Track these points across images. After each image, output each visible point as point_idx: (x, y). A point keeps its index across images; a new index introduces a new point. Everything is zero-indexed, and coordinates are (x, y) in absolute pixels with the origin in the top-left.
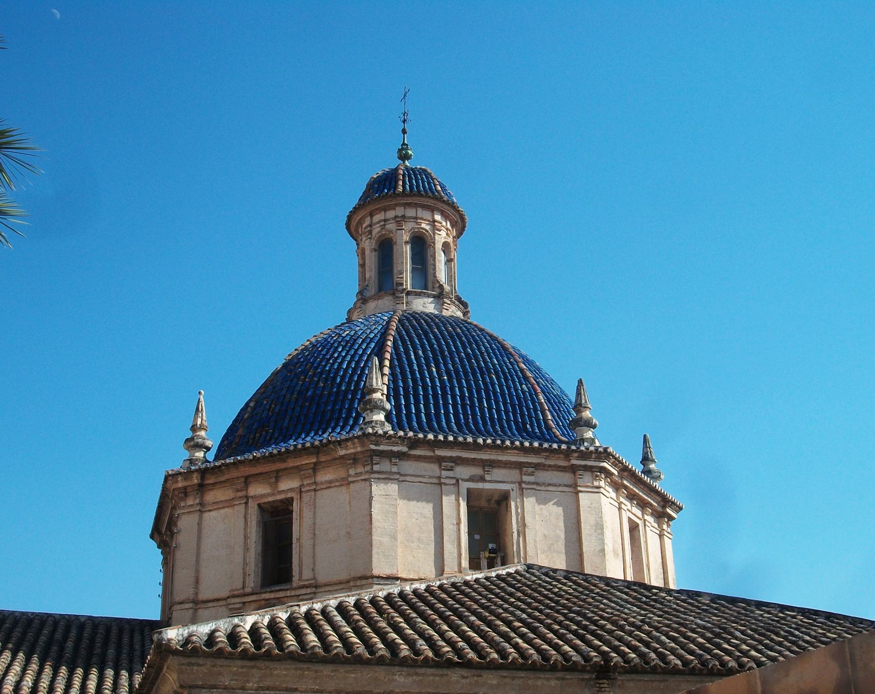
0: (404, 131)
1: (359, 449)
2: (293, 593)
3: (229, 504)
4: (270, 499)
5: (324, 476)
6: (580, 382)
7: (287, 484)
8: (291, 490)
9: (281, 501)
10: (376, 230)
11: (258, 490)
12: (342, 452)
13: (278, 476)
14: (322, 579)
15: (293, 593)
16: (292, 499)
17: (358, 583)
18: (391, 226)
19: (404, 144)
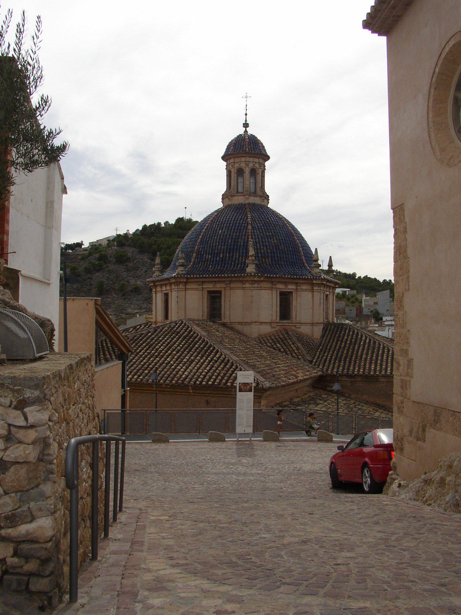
0: (246, 114)
1: (320, 282)
2: (294, 324)
3: (271, 289)
4: (285, 290)
5: (304, 287)
6: (331, 257)
7: (291, 287)
8: (293, 289)
9: (287, 292)
10: (251, 165)
11: (281, 286)
12: (314, 282)
13: (288, 283)
14: (302, 321)
15: (294, 324)
16: (292, 292)
17: (316, 325)
18: (257, 165)
19: (246, 121)
